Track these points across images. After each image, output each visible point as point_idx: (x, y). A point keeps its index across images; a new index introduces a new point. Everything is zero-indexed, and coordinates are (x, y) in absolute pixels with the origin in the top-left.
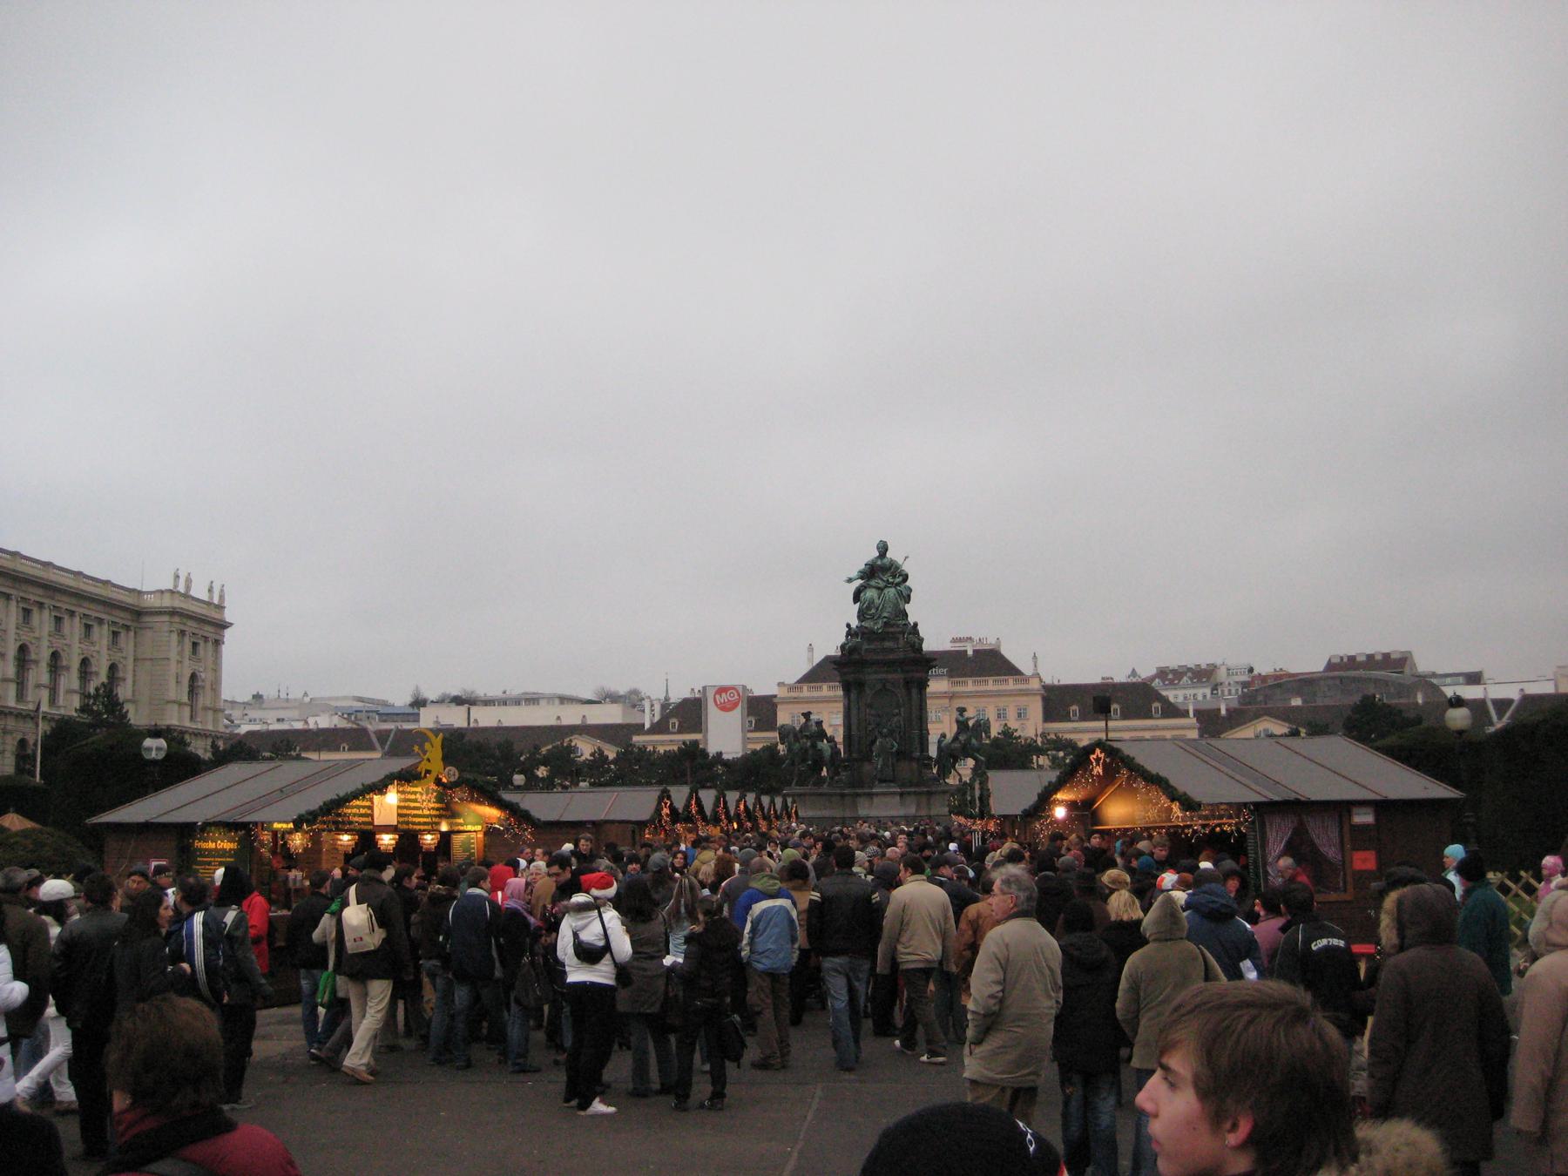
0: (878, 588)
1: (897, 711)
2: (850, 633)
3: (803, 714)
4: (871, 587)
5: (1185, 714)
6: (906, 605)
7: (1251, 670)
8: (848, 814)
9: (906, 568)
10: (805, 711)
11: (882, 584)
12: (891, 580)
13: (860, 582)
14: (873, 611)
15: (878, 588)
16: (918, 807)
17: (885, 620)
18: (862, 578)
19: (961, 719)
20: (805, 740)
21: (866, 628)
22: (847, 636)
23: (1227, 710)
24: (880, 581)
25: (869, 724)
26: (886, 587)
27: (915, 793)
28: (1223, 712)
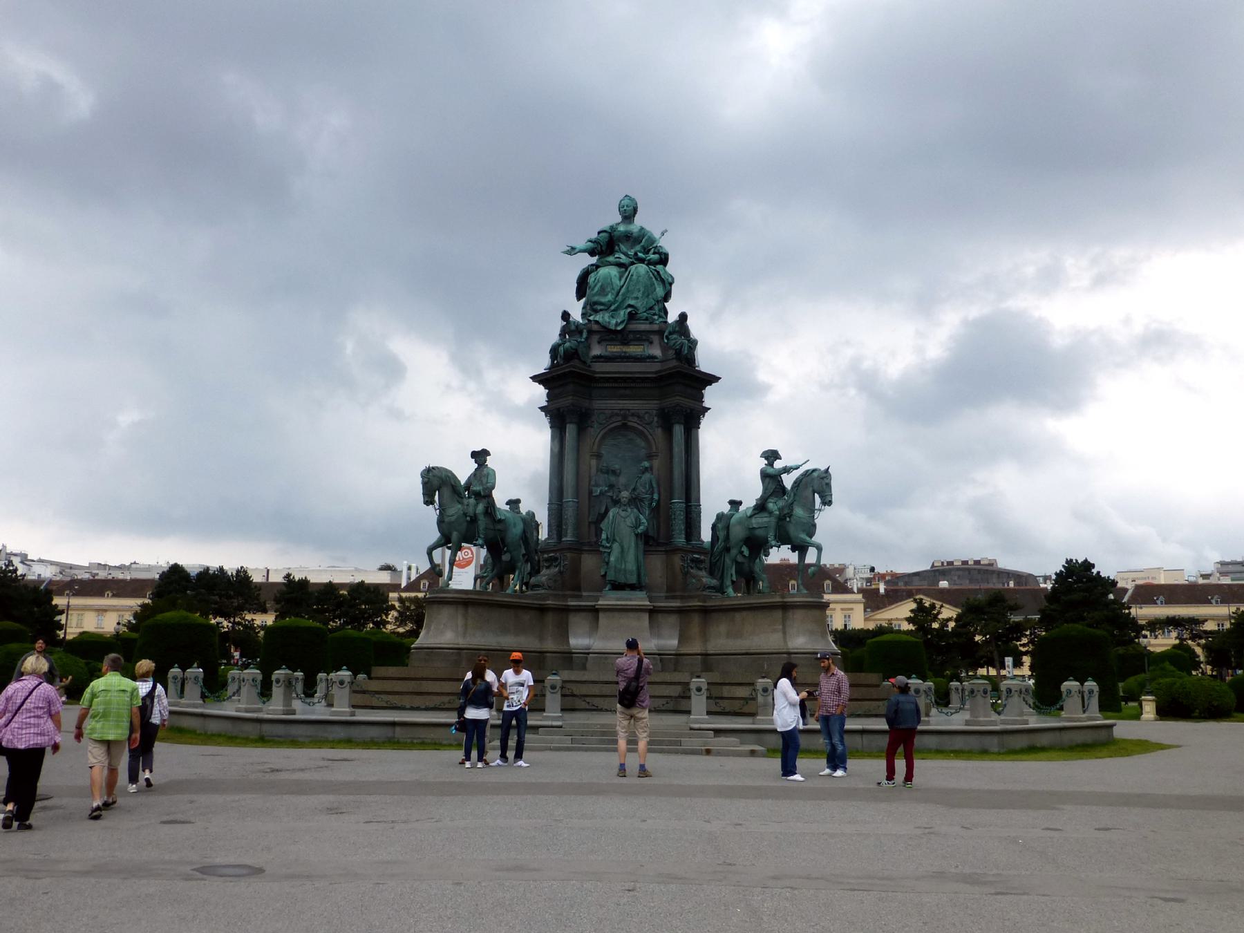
0: (620, 265)
1: (646, 464)
2: (568, 328)
3: (475, 455)
4: (610, 264)
5: (850, 591)
6: (666, 304)
7: (872, 569)
8: (550, 645)
9: (665, 244)
10: (478, 449)
11: (624, 259)
12: (640, 255)
13: (588, 260)
14: (610, 297)
15: (620, 265)
16: (683, 639)
17: (629, 310)
18: (592, 253)
19: (770, 470)
20: (472, 501)
21: (597, 322)
22: (562, 335)
23: (885, 589)
24: (622, 256)
25: (597, 485)
26: (632, 263)
27: (680, 611)
28: (882, 591)
